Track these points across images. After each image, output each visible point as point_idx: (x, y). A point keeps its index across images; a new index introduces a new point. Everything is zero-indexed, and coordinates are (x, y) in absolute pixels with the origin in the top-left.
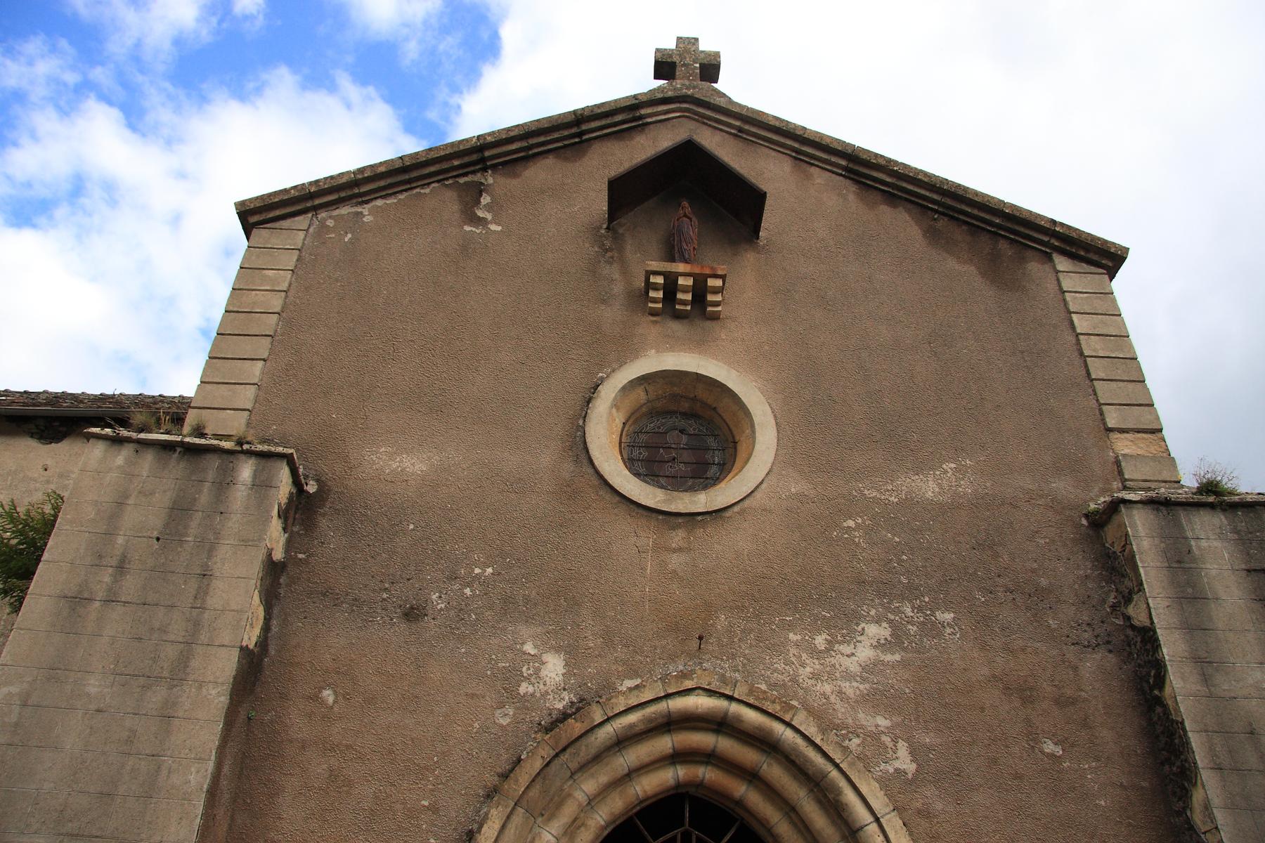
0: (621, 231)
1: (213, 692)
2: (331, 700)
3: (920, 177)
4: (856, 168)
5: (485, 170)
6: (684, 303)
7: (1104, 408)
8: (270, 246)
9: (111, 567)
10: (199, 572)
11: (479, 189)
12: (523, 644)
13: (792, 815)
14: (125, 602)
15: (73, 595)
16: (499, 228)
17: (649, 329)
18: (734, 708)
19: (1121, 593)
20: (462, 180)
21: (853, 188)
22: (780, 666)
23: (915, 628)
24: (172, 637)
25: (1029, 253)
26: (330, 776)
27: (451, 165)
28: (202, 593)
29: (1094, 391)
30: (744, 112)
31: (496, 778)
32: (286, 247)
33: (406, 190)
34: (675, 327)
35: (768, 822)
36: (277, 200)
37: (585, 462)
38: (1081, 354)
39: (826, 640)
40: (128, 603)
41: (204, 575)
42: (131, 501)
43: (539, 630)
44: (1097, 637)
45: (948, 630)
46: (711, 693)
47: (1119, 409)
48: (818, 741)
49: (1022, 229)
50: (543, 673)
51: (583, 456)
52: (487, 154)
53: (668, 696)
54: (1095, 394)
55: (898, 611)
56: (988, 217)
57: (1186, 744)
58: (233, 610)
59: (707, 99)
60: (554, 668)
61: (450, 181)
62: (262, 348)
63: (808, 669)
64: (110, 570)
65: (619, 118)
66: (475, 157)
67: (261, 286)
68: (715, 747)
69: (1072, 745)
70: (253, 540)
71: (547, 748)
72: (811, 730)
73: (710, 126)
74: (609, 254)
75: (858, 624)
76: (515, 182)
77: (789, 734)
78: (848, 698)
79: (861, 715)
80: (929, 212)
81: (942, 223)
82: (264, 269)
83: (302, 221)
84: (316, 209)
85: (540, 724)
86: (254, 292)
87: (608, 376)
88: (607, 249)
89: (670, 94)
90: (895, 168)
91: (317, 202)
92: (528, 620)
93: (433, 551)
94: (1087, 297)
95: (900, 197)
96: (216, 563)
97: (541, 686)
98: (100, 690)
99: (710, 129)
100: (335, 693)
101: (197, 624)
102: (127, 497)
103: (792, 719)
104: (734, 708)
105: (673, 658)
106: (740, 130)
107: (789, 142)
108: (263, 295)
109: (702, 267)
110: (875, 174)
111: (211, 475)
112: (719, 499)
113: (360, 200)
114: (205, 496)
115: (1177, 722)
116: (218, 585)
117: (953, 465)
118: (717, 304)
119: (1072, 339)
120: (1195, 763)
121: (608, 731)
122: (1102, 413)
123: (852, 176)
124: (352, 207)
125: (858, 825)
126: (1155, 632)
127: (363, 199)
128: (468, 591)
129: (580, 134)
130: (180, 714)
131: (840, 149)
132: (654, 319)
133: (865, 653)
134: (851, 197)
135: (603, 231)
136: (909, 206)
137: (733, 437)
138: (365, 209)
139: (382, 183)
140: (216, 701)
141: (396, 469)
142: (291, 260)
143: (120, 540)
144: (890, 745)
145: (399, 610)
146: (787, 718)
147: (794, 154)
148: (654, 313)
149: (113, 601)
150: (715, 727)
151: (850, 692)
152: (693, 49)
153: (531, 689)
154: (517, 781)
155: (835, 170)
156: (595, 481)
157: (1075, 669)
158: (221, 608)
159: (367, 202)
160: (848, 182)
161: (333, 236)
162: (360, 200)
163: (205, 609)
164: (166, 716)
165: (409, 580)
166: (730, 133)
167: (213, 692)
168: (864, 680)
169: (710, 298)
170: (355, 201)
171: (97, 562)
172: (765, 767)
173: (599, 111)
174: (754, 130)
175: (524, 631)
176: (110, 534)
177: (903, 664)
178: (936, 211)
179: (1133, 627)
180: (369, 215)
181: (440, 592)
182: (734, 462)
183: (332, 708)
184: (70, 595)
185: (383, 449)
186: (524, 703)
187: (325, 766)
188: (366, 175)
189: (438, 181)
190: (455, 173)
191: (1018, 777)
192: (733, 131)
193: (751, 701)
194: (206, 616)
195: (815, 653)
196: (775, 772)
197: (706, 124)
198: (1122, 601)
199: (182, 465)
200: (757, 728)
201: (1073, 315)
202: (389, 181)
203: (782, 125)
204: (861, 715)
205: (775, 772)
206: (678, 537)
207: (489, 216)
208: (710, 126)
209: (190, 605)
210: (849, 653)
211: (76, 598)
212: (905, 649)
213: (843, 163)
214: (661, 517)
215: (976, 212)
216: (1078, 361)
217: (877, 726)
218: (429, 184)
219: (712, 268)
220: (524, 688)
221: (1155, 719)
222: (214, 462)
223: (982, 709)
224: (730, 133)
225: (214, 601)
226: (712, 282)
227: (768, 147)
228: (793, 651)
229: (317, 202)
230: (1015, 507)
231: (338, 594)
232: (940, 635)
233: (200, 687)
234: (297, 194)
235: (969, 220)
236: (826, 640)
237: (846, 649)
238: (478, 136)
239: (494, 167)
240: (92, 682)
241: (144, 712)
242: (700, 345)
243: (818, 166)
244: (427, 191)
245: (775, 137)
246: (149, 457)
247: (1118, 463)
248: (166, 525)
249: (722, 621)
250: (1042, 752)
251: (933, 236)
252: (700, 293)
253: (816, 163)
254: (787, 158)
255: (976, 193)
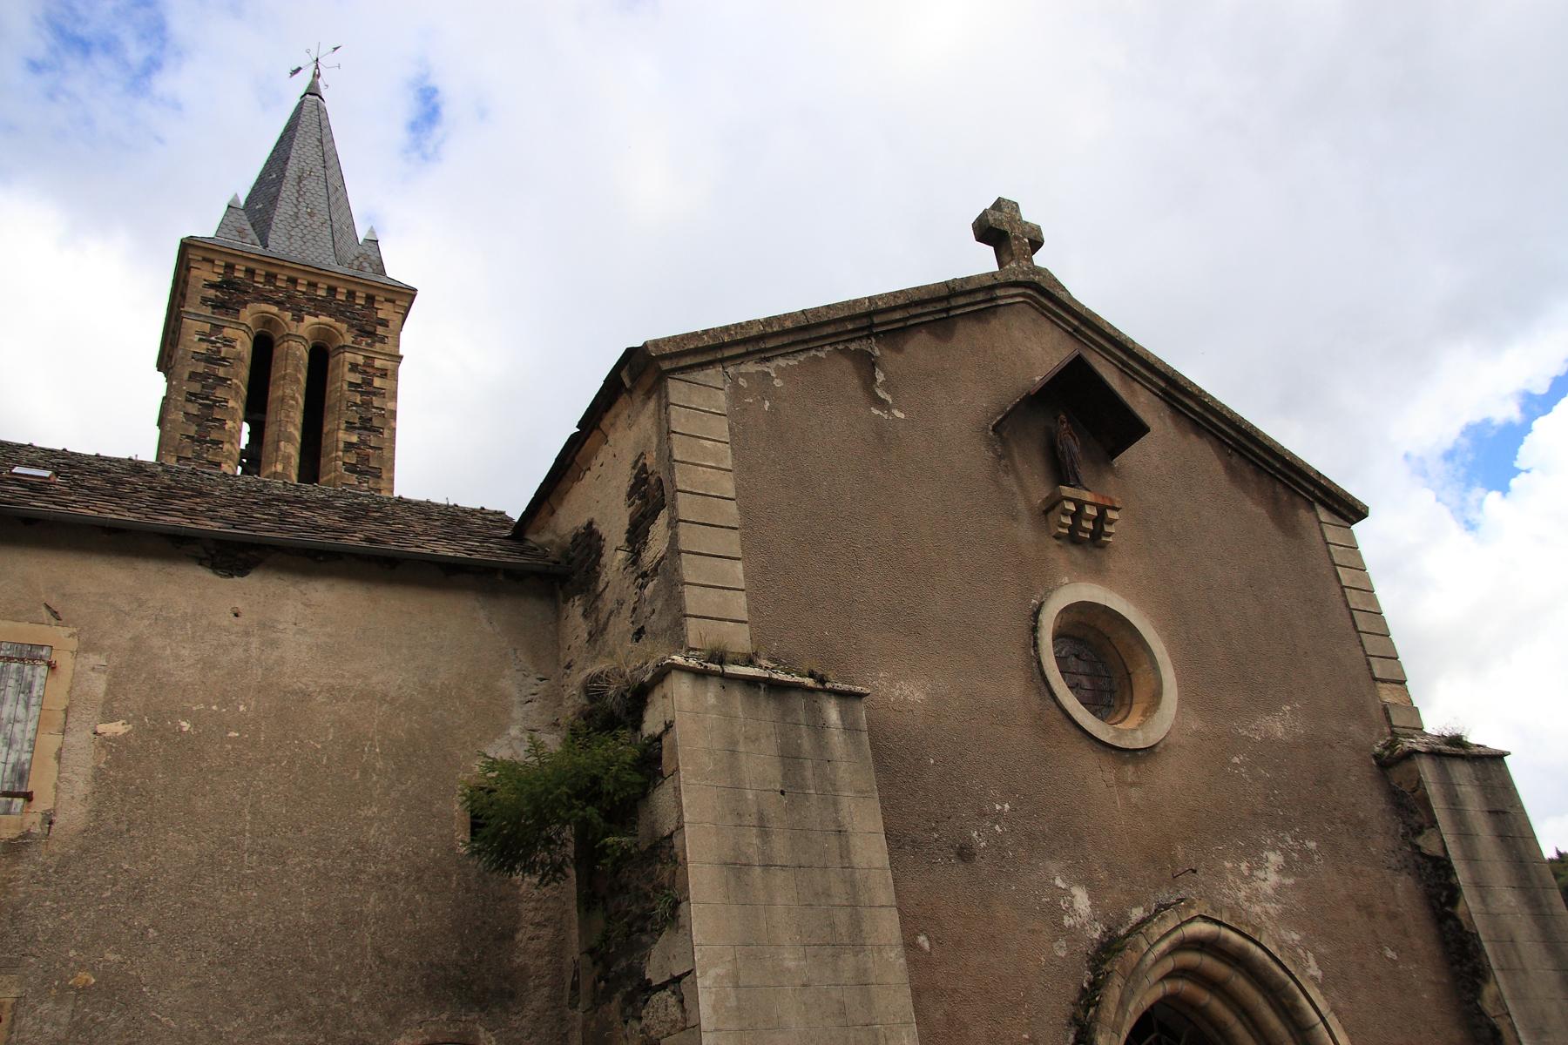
0: (1004, 434)
1: (893, 955)
2: (926, 945)
3: (1224, 413)
4: (1173, 391)
5: (868, 337)
6: (1085, 530)
7: (1371, 659)
8: (694, 406)
9: (754, 826)
10: (833, 828)
11: (867, 364)
12: (1054, 879)
13: (1244, 1018)
14: (781, 866)
15: (733, 860)
16: (902, 416)
17: (1060, 556)
18: (1225, 932)
19: (1409, 825)
20: (853, 346)
21: (1168, 412)
22: (1226, 891)
23: (1297, 856)
24: (837, 901)
25: (1298, 500)
26: (948, 1020)
27: (845, 329)
28: (845, 853)
29: (1361, 641)
30: (1084, 313)
31: (1072, 1007)
32: (713, 410)
33: (802, 350)
34: (1076, 553)
35: (1225, 1024)
36: (692, 346)
37: (1047, 695)
38: (1347, 605)
39: (1247, 866)
40: (784, 866)
41: (840, 831)
42: (741, 748)
43: (1062, 864)
44: (1399, 861)
45: (1316, 857)
46: (1206, 919)
47: (1379, 661)
48: (1279, 957)
49: (1294, 476)
50: (1076, 906)
51: (1044, 688)
52: (876, 320)
53: (1183, 924)
54: (1362, 645)
55: (1283, 841)
56: (1271, 460)
57: (1479, 949)
58: (877, 868)
59: (1051, 290)
60: (1081, 899)
61: (840, 347)
62: (731, 543)
63: (1243, 893)
64: (754, 830)
65: (980, 297)
66: (865, 322)
67: (704, 461)
68: (1201, 964)
69: (1401, 951)
70: (867, 792)
71: (1120, 978)
72: (1273, 948)
73: (1048, 318)
74: (1003, 462)
75: (1262, 853)
76: (900, 358)
77: (1259, 952)
78: (1273, 917)
79: (1283, 932)
80: (1225, 446)
81: (1235, 459)
82: (699, 437)
83: (713, 375)
84: (722, 361)
85: (1088, 954)
86: (700, 468)
87: (1042, 604)
88: (1000, 456)
89: (1021, 278)
90: (1206, 400)
91: (727, 353)
92: (1052, 855)
93: (957, 786)
94: (1341, 551)
95: (1203, 427)
96: (844, 818)
97: (1078, 918)
98: (797, 963)
99: (1048, 321)
100: (929, 939)
101: (853, 885)
102: (736, 743)
103: (1260, 939)
104: (1225, 932)
105: (1158, 887)
106: (1076, 329)
107: (1119, 353)
108: (711, 473)
109: (1103, 498)
110: (1187, 401)
111: (802, 716)
112: (1151, 735)
113: (763, 356)
114: (807, 744)
115: (1473, 934)
116: (856, 842)
117: (1288, 708)
118: (1109, 535)
119: (1338, 590)
120: (1489, 965)
121: (1151, 957)
122: (1369, 664)
123: (1167, 399)
124: (756, 363)
125: (1310, 1025)
126: (1450, 862)
127: (765, 356)
128: (997, 827)
129: (947, 310)
130: (874, 981)
131: (1163, 370)
132: (1058, 543)
133: (1273, 878)
134: (1169, 422)
135: (991, 434)
136: (1212, 438)
137: (1127, 670)
138: (770, 368)
139: (786, 340)
140: (897, 963)
141: (897, 699)
142: (721, 428)
143: (750, 795)
144: (1303, 955)
145: (952, 851)
146: (1257, 939)
147: (1120, 366)
148: (1058, 537)
149: (771, 866)
150: (1198, 946)
151: (1271, 911)
152: (1018, 218)
153: (1072, 922)
154: (1108, 1009)
155: (1154, 389)
156: (1059, 715)
157: (1393, 888)
158: (866, 866)
159: (768, 360)
160: (1162, 404)
161: (751, 401)
162: (763, 356)
163: (852, 868)
164: (862, 983)
165: (949, 818)
166: (1067, 331)
167: (893, 955)
168: (1278, 901)
169: (1107, 529)
170: (758, 356)
171: (738, 822)
172: (1234, 979)
173: (968, 288)
174: (1089, 333)
175: (1053, 866)
176: (737, 787)
177: (1296, 886)
178: (1230, 446)
179: (1423, 855)
180: (777, 378)
181: (978, 830)
182: (1132, 694)
183: (930, 953)
184: (728, 861)
185: (881, 675)
186: (1072, 934)
187: (941, 1012)
188: (775, 329)
189: (831, 345)
190: (846, 338)
191: (1377, 978)
192: (1069, 329)
193: (1234, 925)
194: (857, 875)
195: (1247, 879)
196: (1241, 984)
197: (1045, 316)
198: (1411, 833)
199: (772, 704)
200: (1237, 947)
201: (1338, 568)
202: (792, 338)
203: (1116, 334)
204: (1283, 932)
205: (1241, 984)
206: (1129, 772)
207: (889, 398)
208: (1048, 318)
209: (840, 866)
210: (1262, 877)
211: (736, 864)
212: (1295, 875)
213: (1163, 384)
214: (1113, 752)
215: (1262, 454)
216: (1346, 612)
217: (1293, 940)
218: (822, 346)
219: (1110, 500)
220: (1068, 921)
221: (1446, 929)
222: (799, 702)
223: (1348, 923)
224: (1067, 331)
225: (858, 860)
226: (1111, 514)
227: (1099, 353)
228: (1230, 877)
229: (727, 353)
230: (1332, 747)
231: (897, 836)
232: (1311, 862)
233: (880, 952)
234: (711, 343)
235: (1254, 459)
236: (1247, 866)
237: (1261, 874)
238: (869, 298)
239: (876, 335)
240: (786, 955)
241: (843, 982)
242: (1098, 573)
243: (1139, 382)
244: (822, 354)
245: (1107, 345)
246: (737, 696)
247: (1386, 710)
248: (785, 776)
249: (1180, 850)
250: (1387, 958)
251: (1230, 469)
252: (1101, 519)
253: (1139, 379)
254: (1115, 369)
255: (1266, 437)
